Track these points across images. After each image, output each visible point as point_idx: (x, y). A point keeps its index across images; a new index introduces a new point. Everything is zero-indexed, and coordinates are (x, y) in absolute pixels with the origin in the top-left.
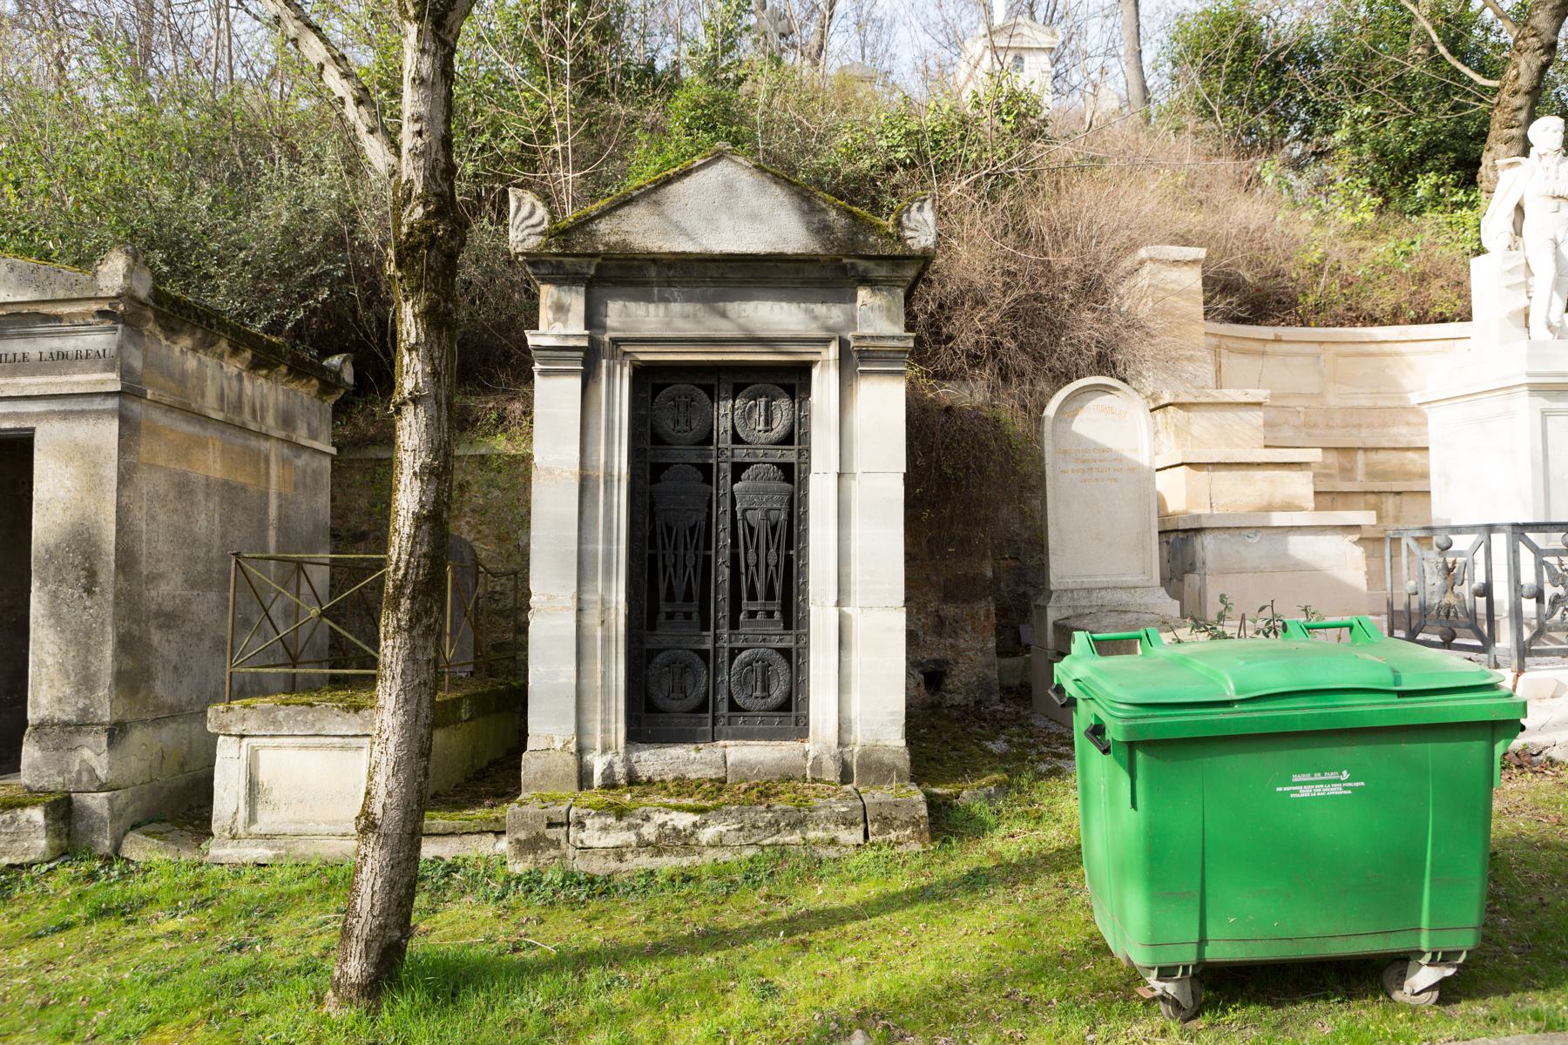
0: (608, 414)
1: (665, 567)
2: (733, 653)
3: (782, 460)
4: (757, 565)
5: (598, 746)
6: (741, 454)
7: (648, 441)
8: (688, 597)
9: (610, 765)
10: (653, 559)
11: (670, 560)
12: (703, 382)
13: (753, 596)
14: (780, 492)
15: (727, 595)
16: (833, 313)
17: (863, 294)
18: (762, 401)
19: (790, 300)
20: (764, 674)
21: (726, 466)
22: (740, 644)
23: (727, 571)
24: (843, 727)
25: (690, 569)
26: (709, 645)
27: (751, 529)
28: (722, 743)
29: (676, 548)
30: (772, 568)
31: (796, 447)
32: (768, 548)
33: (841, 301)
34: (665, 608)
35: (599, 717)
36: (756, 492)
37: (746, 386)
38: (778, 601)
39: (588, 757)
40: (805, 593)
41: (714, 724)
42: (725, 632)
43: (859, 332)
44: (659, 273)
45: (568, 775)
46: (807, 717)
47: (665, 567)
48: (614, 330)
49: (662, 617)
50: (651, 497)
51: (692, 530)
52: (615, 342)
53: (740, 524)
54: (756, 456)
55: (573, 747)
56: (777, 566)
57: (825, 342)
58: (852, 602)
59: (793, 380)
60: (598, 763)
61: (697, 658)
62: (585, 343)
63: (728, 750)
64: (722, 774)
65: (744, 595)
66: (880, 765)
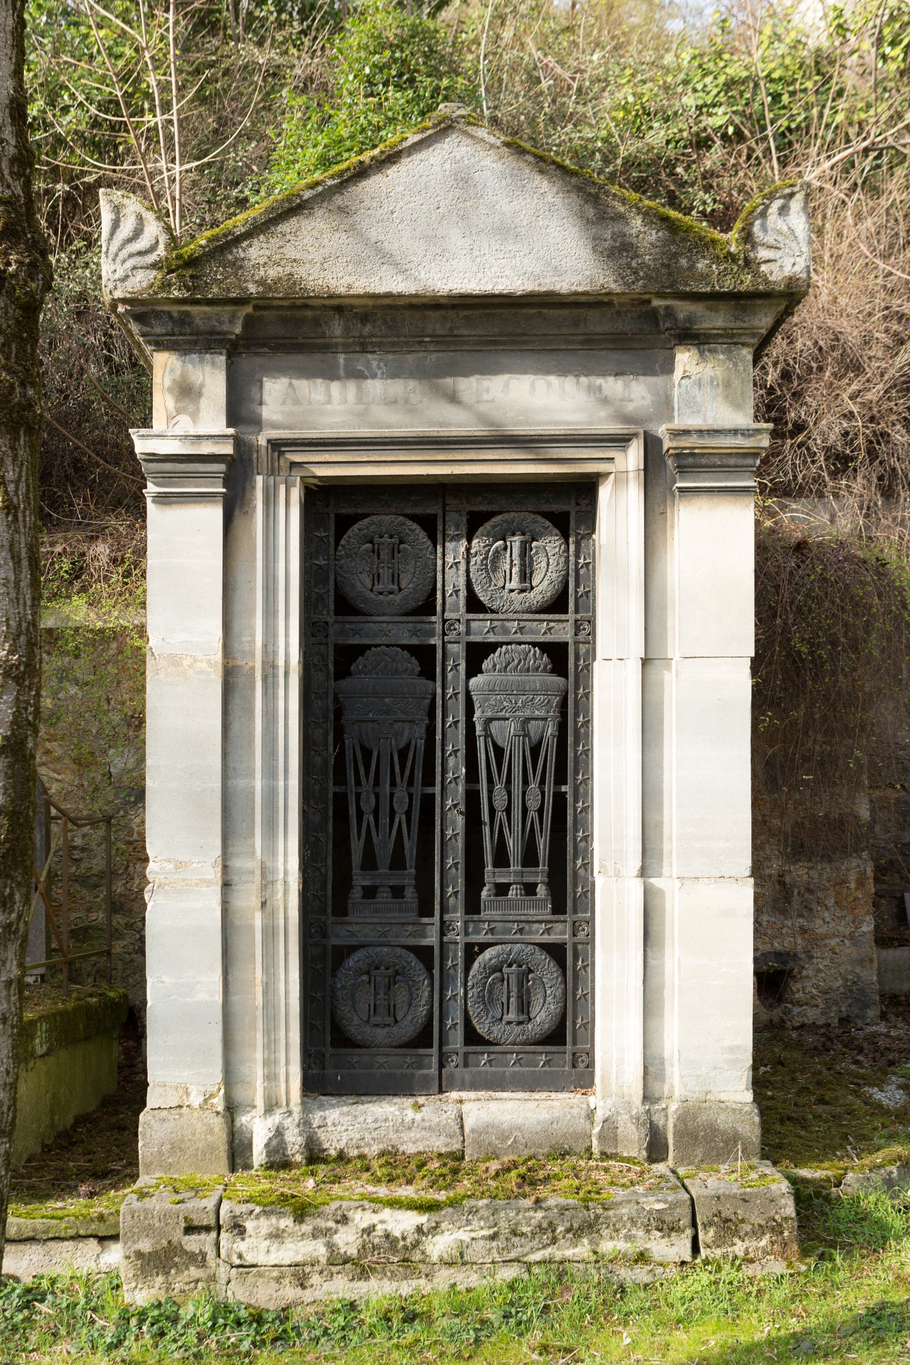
0: (266, 568)
1: (360, 814)
2: (472, 952)
3: (549, 638)
4: (508, 810)
5: (260, 1102)
6: (482, 629)
7: (328, 603)
8: (398, 863)
9: (279, 1132)
10: (341, 801)
11: (368, 805)
12: (418, 511)
13: (501, 860)
14: (546, 690)
15: (461, 859)
16: (634, 392)
17: (685, 359)
18: (516, 542)
19: (563, 372)
20: (520, 985)
21: (458, 650)
22: (481, 938)
23: (460, 821)
24: (652, 1070)
25: (400, 817)
26: (432, 939)
27: (499, 752)
28: (454, 1095)
29: (377, 783)
30: (532, 814)
31: (571, 616)
32: (526, 782)
33: (648, 371)
34: (360, 880)
35: (259, 1055)
36: (507, 690)
37: (487, 516)
38: (543, 868)
39: (243, 1119)
40: (587, 855)
41: (441, 1066)
42: (457, 918)
43: (678, 423)
44: (347, 330)
45: (212, 1148)
46: (590, 1053)
47: (360, 814)
48: (275, 426)
49: (356, 894)
50: (336, 698)
51: (403, 753)
52: (276, 445)
53: (481, 744)
54: (506, 631)
55: (219, 1103)
56: (540, 811)
57: (621, 441)
58: (665, 870)
59: (567, 504)
60: (259, 1129)
61: (412, 958)
62: (227, 449)
63: (465, 1108)
64: (456, 1146)
65: (489, 858)
66: (712, 1130)
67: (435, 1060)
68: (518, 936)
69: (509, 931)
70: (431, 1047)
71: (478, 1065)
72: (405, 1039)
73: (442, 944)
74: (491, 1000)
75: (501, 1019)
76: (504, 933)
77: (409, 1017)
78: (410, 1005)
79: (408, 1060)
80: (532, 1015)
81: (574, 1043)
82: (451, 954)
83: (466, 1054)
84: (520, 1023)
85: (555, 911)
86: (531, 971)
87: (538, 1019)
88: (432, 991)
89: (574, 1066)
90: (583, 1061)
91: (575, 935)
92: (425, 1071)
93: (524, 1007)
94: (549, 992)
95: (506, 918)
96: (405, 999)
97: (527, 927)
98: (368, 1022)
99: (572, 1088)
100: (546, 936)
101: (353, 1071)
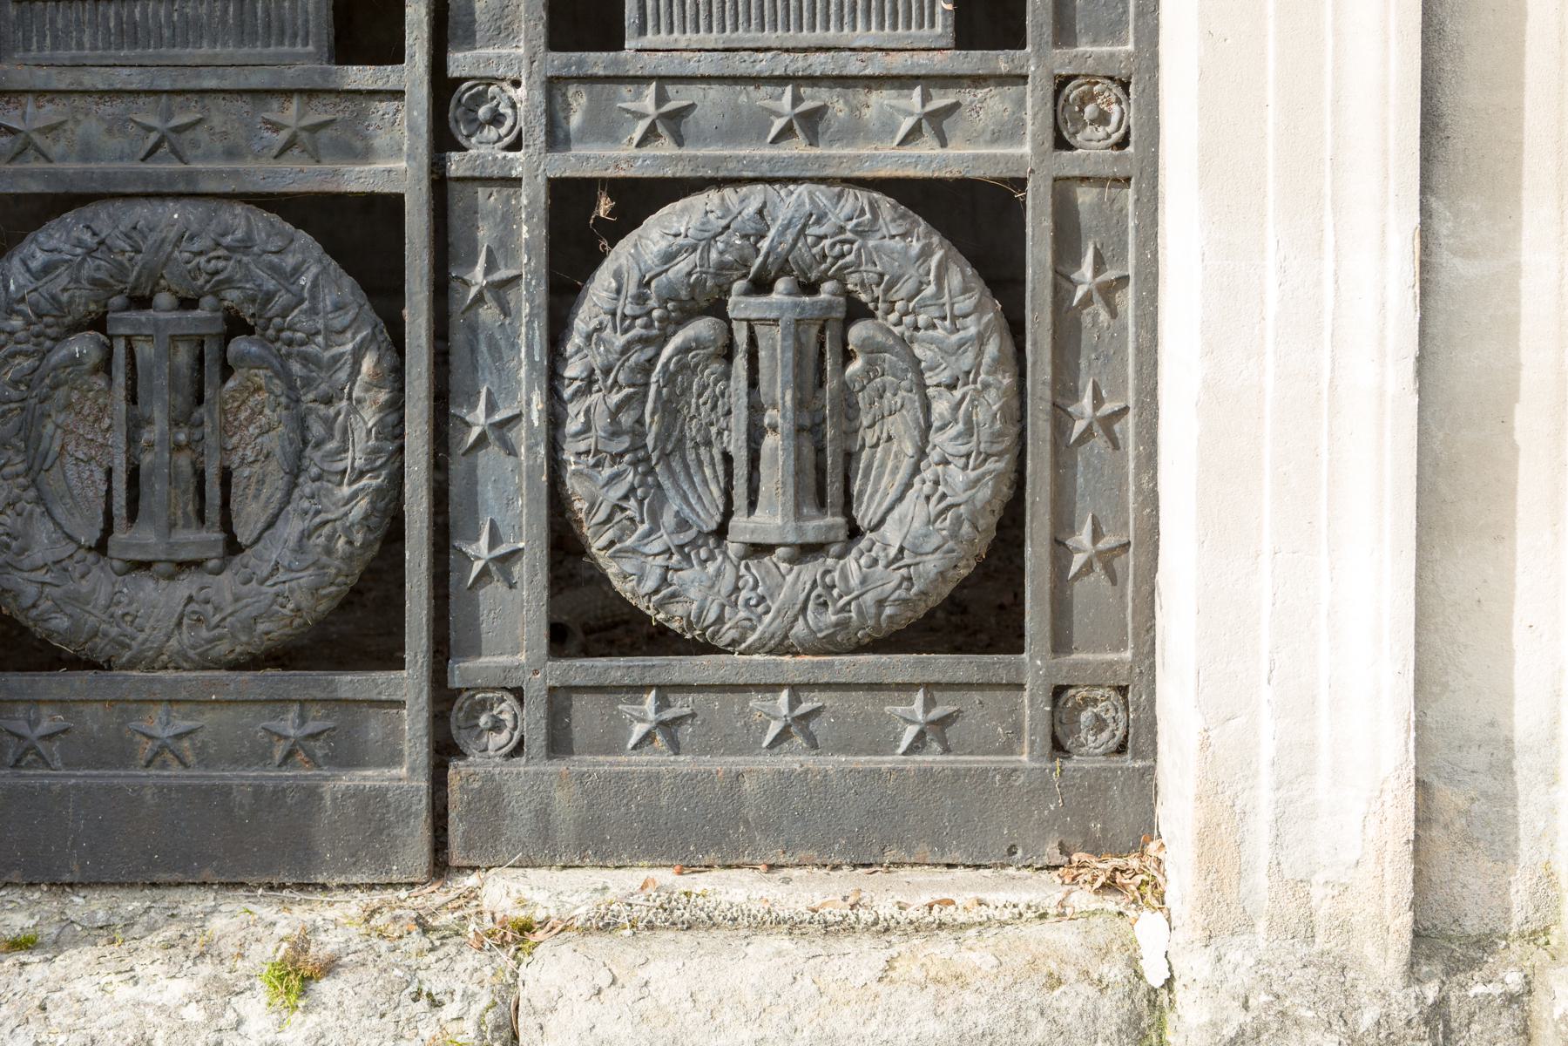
2: (583, 224)
20: (811, 374)
26: (393, 164)
28: (502, 891)
41: (444, 750)
46: (1134, 691)
61: (305, 254)
67: (413, 725)
68: (797, 148)
69: (749, 127)
70: (393, 659)
71: (612, 746)
72: (272, 630)
73: (440, 184)
74: (673, 446)
75: (721, 532)
76: (731, 133)
77: (291, 528)
78: (295, 473)
79: (289, 724)
80: (865, 514)
81: (1061, 642)
82: (485, 234)
83: (559, 699)
84: (807, 551)
85: (967, 35)
86: (856, 311)
87: (892, 534)
88: (397, 405)
89: (1058, 747)
90: (1100, 724)
91: (1061, 143)
92: (369, 777)
93: (828, 479)
94: (940, 407)
95: (741, 64)
96: (272, 442)
97: (837, 103)
98: (101, 547)
99: (1052, 853)
100: (927, 148)
101: (34, 776)
